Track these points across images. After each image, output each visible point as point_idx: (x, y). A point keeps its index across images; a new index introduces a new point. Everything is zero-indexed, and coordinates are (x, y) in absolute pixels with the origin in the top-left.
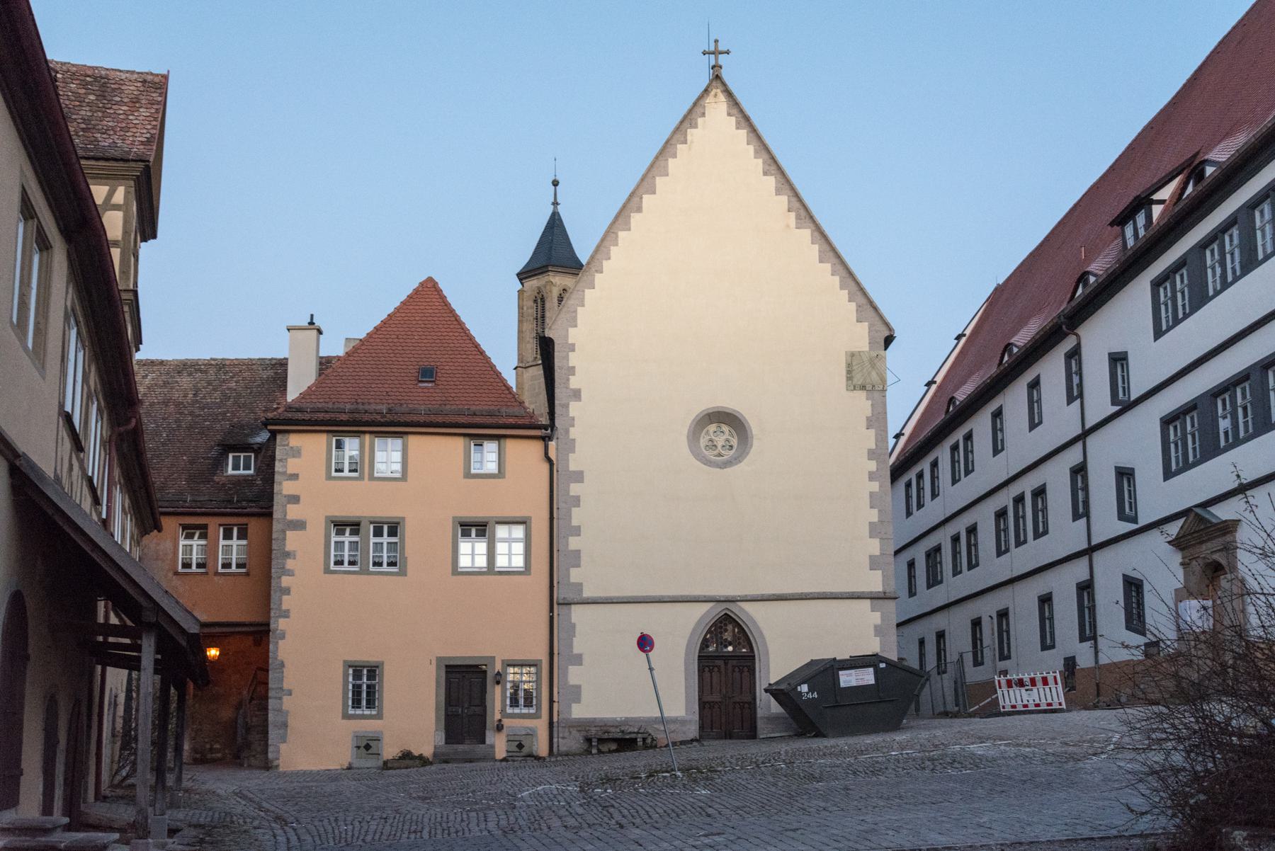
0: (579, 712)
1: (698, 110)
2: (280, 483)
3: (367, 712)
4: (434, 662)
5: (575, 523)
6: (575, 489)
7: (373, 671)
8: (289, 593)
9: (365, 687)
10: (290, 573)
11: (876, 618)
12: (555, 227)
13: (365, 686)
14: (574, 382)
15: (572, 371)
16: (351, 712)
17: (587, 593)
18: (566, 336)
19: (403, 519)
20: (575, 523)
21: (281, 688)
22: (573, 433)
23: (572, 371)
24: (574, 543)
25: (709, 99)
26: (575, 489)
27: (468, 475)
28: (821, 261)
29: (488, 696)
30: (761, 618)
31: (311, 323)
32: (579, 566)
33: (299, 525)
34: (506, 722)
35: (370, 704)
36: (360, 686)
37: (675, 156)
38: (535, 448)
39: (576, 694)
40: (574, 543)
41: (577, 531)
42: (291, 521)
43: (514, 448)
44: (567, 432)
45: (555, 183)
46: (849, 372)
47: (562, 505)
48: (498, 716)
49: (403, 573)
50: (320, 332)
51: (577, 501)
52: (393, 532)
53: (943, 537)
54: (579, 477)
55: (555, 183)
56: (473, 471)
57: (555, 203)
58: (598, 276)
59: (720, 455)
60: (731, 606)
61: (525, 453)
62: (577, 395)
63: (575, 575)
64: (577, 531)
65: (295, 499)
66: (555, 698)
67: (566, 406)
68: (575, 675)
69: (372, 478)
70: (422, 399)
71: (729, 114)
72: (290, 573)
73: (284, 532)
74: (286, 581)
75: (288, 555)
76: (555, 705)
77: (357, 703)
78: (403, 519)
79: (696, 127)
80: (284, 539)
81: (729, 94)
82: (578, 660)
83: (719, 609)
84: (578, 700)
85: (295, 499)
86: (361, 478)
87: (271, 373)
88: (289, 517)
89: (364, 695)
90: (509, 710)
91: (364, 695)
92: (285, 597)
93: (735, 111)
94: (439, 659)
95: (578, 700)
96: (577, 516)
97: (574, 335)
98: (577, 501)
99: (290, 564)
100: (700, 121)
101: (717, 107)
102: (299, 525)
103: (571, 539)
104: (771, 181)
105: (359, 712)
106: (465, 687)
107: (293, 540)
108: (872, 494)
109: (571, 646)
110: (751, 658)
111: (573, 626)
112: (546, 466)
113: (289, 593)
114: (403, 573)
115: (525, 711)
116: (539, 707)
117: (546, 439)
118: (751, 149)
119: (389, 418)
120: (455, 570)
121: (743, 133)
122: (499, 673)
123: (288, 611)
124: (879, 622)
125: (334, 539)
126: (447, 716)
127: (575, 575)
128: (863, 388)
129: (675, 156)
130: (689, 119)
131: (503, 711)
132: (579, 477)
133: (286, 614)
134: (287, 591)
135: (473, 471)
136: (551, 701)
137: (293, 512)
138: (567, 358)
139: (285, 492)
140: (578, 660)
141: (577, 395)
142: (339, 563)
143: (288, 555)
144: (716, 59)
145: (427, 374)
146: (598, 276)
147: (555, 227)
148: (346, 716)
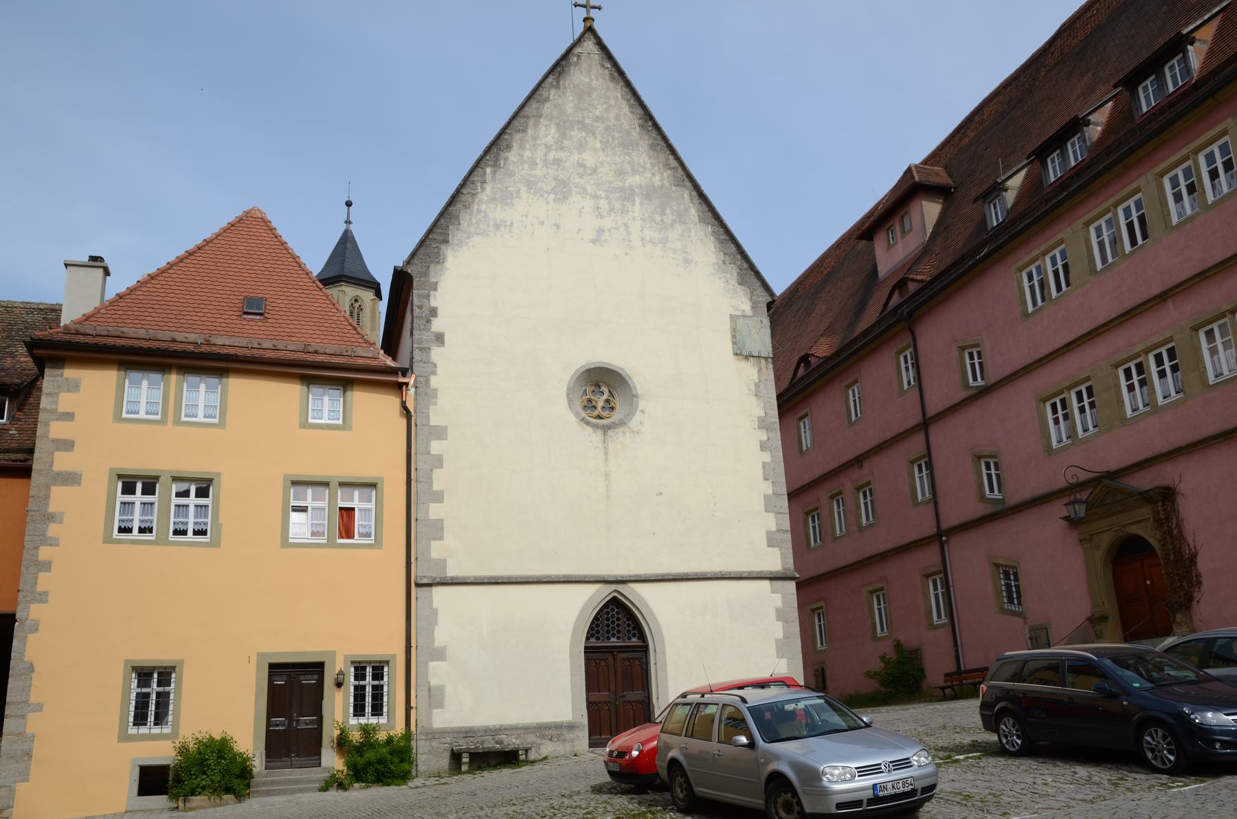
0: (442, 719)
2: (47, 424)
3: (156, 730)
4: (254, 659)
5: (436, 487)
6: (436, 447)
7: (165, 674)
8: (48, 570)
9: (154, 696)
10: (54, 543)
11: (777, 600)
12: (347, 243)
13: (152, 692)
14: (437, 325)
16: (133, 731)
17: (452, 572)
19: (219, 474)
20: (436, 487)
21: (26, 703)
22: (434, 381)
24: (435, 511)
26: (436, 447)
27: (305, 425)
29: (325, 703)
30: (653, 602)
32: (441, 538)
33: (71, 479)
35: (160, 719)
36: (148, 695)
39: (436, 698)
40: (435, 511)
41: (439, 497)
42: (59, 474)
43: (362, 399)
44: (428, 381)
45: (349, 204)
46: (734, 337)
47: (421, 465)
49: (215, 544)
50: (107, 272)
51: (439, 461)
52: (202, 493)
54: (440, 433)
55: (349, 204)
56: (311, 421)
57: (348, 222)
59: (599, 417)
60: (620, 588)
62: (440, 338)
63: (437, 550)
64: (439, 497)
65: (68, 445)
66: (413, 704)
68: (436, 673)
69: (178, 422)
72: (54, 543)
73: (48, 487)
74: (44, 553)
75: (51, 518)
76: (413, 712)
77: (140, 719)
78: (219, 474)
80: (48, 497)
81: (600, 44)
82: (440, 655)
83: (600, 594)
84: (440, 705)
85: (68, 445)
86: (163, 421)
88: (57, 467)
89: (152, 707)
91: (152, 707)
92: (41, 575)
94: (260, 656)
95: (440, 705)
98: (439, 461)
99: (53, 529)
102: (71, 479)
103: (432, 505)
105: (143, 730)
106: (293, 689)
107: (59, 498)
108: (764, 465)
109: (431, 637)
110: (645, 649)
111: (435, 613)
112: (404, 421)
113: (48, 570)
114: (215, 544)
119: (205, 349)
120: (285, 543)
122: (341, 673)
123: (46, 593)
124: (779, 604)
125: (121, 498)
126: (268, 732)
127: (437, 550)
132: (440, 433)
133: (42, 598)
134: (47, 566)
135: (311, 421)
136: (408, 708)
137: (62, 462)
139: (51, 436)
140: (440, 655)
142: (125, 530)
143: (51, 518)
144: (588, 12)
147: (347, 243)
148: (124, 737)
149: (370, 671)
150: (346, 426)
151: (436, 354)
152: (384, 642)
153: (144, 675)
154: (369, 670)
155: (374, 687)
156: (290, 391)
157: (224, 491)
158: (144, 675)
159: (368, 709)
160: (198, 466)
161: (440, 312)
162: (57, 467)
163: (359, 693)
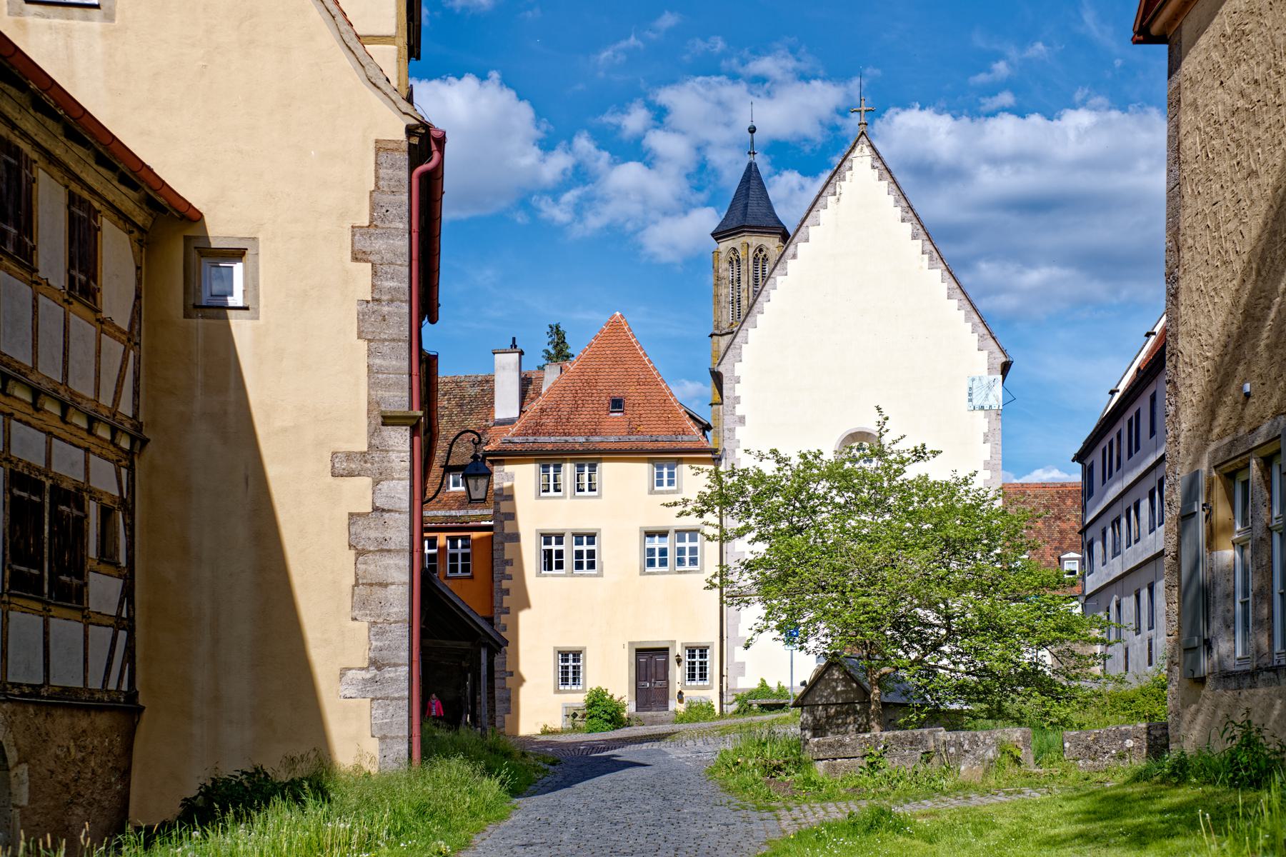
1: (847, 164)
3: (574, 688)
7: (577, 655)
13: (569, 665)
14: (739, 410)
18: (733, 371)
25: (857, 152)
28: (949, 297)
31: (514, 345)
34: (686, 693)
36: (567, 667)
37: (825, 207)
46: (970, 394)
48: (678, 688)
58: (759, 316)
62: (742, 420)
67: (732, 430)
71: (873, 167)
73: (502, 543)
77: (565, 681)
79: (844, 179)
84: (743, 674)
87: (477, 389)
88: (506, 531)
90: (688, 683)
93: (878, 164)
95: (743, 674)
97: (739, 369)
100: (848, 174)
106: (650, 662)
115: (701, 683)
116: (712, 681)
118: (891, 199)
128: (982, 408)
129: (825, 207)
131: (683, 684)
138: (733, 389)
146: (759, 316)
148: (557, 691)
149: (697, 652)
152: (711, 637)
154: (697, 652)
155: (701, 663)
158: (564, 655)
159: (697, 677)
160: (585, 526)
161: (742, 400)
162: (506, 531)
163: (692, 669)
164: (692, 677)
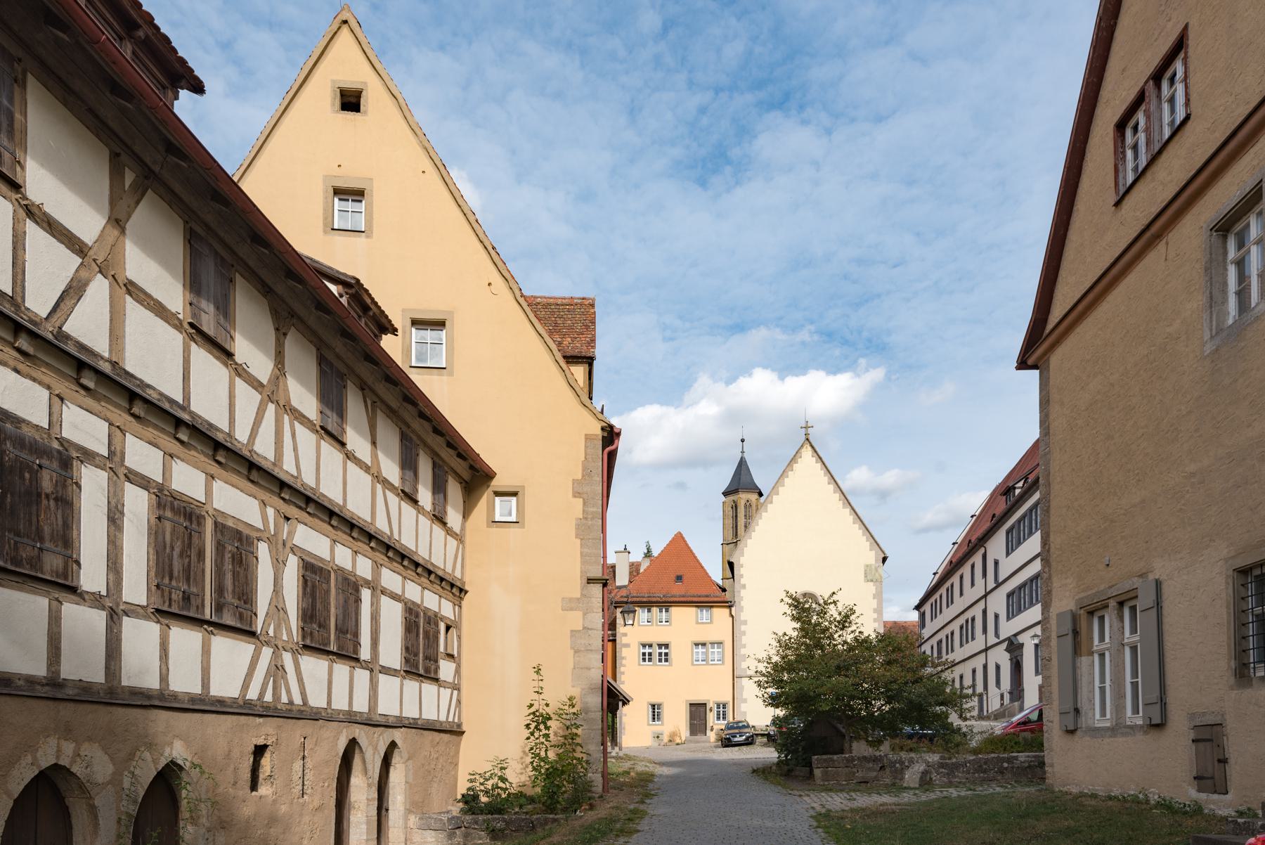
6: (743, 628)
7: (659, 706)
13: (656, 711)
15: (742, 576)
22: (743, 603)
23: (742, 576)
24: (743, 651)
26: (743, 628)
27: (697, 623)
33: (627, 645)
38: (727, 611)
41: (744, 646)
51: (744, 633)
53: (955, 627)
54: (745, 623)
61: (720, 614)
64: (744, 646)
65: (625, 635)
70: (677, 590)
85: (625, 635)
96: (744, 640)
97: (743, 560)
98: (744, 633)
101: (807, 453)
102: (627, 645)
104: (832, 487)
117: (730, 607)
121: (819, 465)
130: (794, 460)
132: (745, 623)
137: (625, 640)
141: (744, 587)
145: (679, 578)
150: (711, 622)
151: (743, 593)
153: (653, 706)
156: (691, 611)
157: (672, 647)
160: (663, 640)
164: (718, 718)
